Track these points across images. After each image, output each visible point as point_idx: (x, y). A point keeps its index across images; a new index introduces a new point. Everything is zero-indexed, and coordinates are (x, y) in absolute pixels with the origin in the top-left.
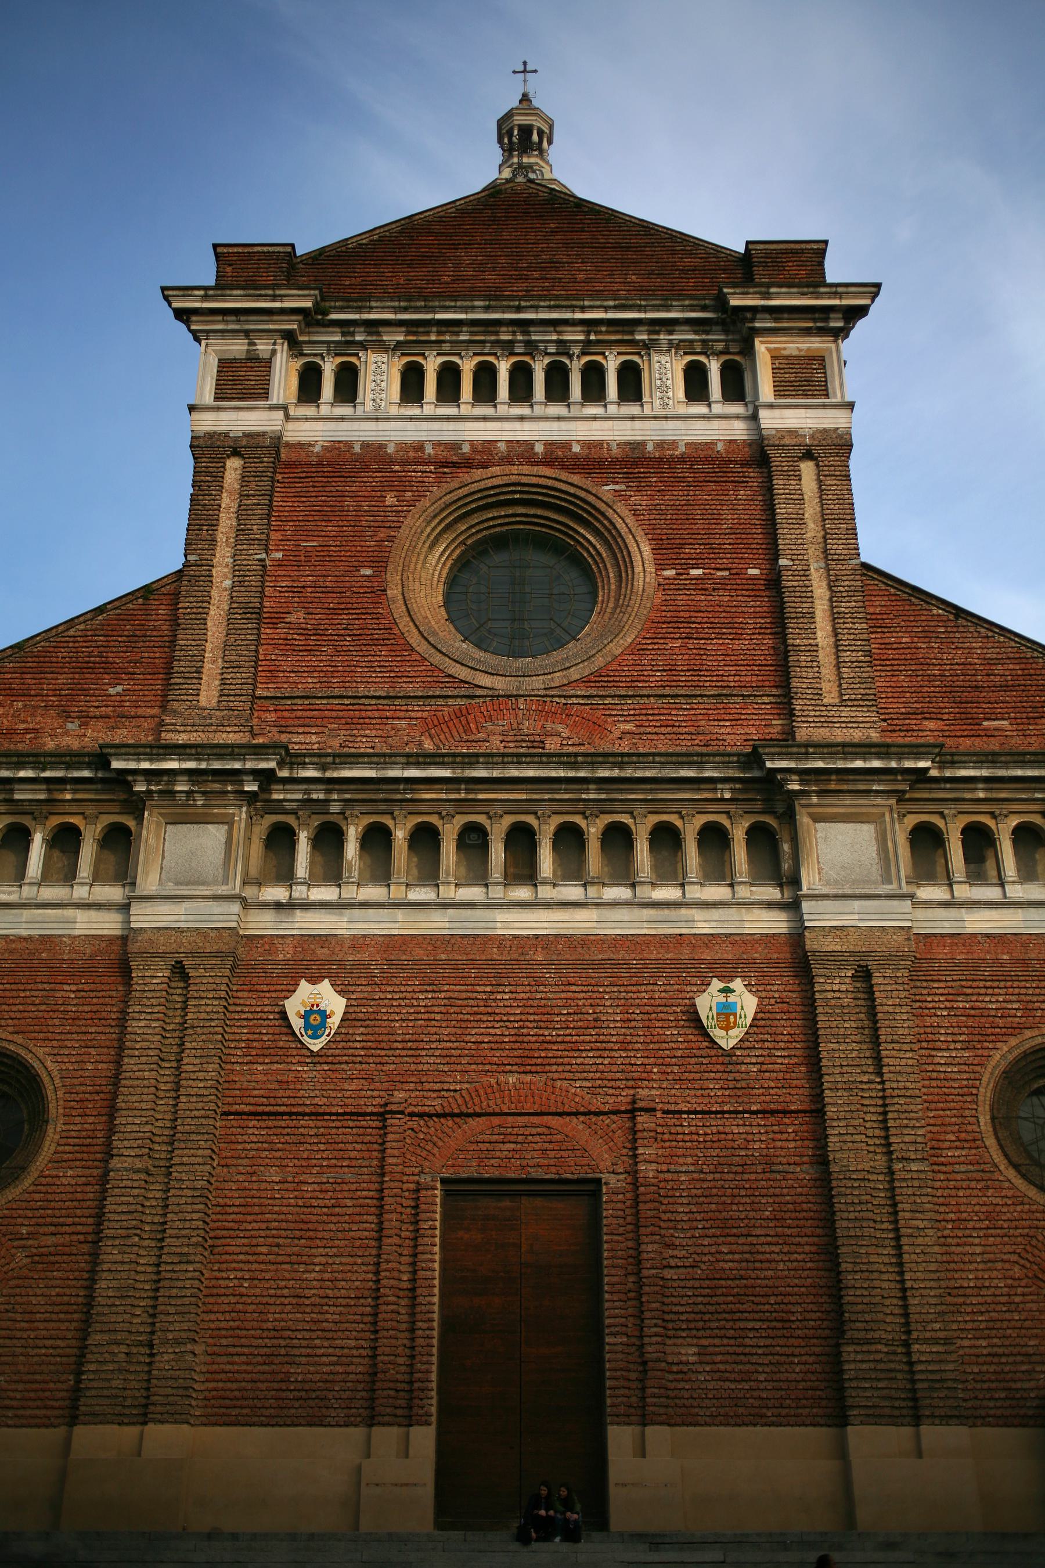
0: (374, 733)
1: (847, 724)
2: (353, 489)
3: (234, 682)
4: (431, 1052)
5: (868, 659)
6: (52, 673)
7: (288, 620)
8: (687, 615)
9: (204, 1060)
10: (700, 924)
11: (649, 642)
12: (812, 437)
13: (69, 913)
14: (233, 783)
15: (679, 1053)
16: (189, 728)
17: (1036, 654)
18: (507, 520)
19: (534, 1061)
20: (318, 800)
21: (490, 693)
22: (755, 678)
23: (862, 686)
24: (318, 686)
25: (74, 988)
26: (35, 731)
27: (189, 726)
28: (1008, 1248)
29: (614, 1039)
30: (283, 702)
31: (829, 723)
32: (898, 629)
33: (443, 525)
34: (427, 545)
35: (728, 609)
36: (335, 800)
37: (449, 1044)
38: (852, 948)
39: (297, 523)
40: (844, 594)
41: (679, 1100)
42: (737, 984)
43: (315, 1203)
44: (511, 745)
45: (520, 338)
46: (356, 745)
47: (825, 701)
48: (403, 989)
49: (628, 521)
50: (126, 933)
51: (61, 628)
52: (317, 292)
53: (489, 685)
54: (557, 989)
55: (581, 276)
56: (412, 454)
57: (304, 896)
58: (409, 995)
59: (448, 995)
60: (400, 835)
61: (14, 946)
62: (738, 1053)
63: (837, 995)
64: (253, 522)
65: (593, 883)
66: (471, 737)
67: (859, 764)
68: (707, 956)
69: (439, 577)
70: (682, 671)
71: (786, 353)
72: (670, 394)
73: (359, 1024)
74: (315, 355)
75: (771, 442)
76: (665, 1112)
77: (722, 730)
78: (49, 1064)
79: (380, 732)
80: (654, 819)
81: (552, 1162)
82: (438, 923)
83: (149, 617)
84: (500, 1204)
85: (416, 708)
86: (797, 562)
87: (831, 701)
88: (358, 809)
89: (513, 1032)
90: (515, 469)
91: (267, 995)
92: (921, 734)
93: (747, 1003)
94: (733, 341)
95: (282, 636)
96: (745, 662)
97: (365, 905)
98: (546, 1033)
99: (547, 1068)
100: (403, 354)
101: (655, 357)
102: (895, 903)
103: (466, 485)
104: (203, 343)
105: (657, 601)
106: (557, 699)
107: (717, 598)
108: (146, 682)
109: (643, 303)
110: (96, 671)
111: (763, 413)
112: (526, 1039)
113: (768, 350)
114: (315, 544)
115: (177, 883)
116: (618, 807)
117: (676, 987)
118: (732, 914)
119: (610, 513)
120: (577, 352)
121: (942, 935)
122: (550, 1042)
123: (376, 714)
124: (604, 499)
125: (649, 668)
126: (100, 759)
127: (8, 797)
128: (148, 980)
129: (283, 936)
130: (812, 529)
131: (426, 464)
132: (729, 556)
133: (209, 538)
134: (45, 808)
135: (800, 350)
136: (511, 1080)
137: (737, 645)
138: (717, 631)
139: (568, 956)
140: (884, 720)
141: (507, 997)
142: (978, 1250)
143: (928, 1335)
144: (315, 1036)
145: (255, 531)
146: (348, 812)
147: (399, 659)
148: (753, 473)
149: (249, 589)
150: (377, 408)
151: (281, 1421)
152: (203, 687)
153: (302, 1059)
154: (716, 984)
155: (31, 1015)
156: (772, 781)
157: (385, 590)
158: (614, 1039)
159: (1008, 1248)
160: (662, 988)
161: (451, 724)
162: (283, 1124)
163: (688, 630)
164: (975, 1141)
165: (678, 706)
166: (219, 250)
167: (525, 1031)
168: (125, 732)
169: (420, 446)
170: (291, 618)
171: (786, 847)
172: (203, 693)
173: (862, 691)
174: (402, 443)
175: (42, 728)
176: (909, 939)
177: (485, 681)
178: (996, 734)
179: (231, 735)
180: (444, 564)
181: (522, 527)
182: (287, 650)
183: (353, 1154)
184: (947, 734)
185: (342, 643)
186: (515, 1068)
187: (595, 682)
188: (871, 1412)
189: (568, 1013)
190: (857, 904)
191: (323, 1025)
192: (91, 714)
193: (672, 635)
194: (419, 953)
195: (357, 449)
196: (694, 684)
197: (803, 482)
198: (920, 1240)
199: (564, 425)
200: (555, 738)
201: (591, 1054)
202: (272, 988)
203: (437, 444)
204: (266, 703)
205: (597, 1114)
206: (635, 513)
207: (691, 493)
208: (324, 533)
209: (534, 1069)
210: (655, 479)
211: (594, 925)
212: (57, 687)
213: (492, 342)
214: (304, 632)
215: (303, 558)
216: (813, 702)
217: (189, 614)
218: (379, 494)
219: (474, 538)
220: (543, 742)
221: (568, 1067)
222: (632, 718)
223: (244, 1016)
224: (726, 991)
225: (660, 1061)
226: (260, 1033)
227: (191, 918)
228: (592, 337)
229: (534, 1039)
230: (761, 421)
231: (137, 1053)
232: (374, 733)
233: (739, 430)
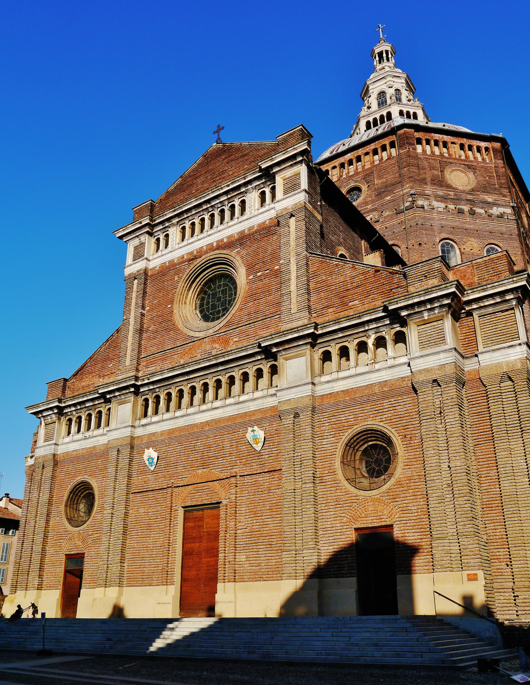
10: (251, 407)
17: (369, 269)
25: (101, 460)
28: (342, 512)
29: (227, 453)
41: (244, 471)
42: (256, 428)
43: (152, 518)
44: (203, 356)
48: (174, 446)
52: (148, 217)
56: (181, 260)
62: (262, 451)
71: (287, 177)
76: (240, 476)
81: (209, 497)
84: (199, 513)
88: (163, 389)
90: (208, 255)
92: (327, 315)
93: (261, 434)
100: (180, 225)
102: (306, 386)
105: (247, 289)
106: (216, 335)
109: (238, 179)
113: (281, 178)
121: (327, 394)
129: (144, 435)
131: (185, 262)
134: (94, 407)
135: (291, 174)
136: (200, 471)
137: (269, 298)
142: (332, 513)
143: (308, 547)
144: (151, 466)
151: (144, 585)
154: (250, 429)
158: (227, 453)
159: (342, 512)
160: (241, 432)
162: (145, 494)
169: (183, 257)
172: (127, 361)
176: (310, 399)
177: (197, 334)
178: (353, 307)
181: (216, 273)
183: (161, 502)
184: (336, 312)
188: (288, 575)
190: (294, 390)
191: (153, 462)
194: (177, 434)
195: (167, 264)
198: (308, 512)
201: (221, 459)
203: (188, 253)
205: (221, 480)
206: (242, 258)
213: (202, 211)
219: (204, 282)
224: (253, 431)
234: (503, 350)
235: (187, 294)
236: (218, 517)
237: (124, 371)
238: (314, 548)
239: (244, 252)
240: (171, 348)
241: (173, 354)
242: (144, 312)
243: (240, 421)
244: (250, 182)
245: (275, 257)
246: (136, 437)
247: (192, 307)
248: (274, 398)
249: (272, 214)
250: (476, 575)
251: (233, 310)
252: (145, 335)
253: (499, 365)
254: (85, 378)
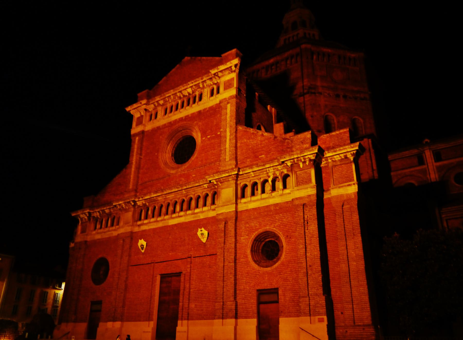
42: (203, 229)
67: (224, 175)
76: (194, 257)
82: (160, 225)
93: (206, 233)
94: (218, 80)
121: (244, 210)
144: (143, 250)
154: (199, 230)
164: (246, 257)
169: (165, 125)
191: (143, 247)
206: (199, 126)
224: (201, 231)
234: (344, 188)
235: (167, 147)
236: (180, 281)
238: (233, 301)
239: (200, 123)
242: (141, 157)
245: (218, 127)
247: (170, 155)
248: (214, 212)
249: (218, 101)
250: (323, 318)
251: (193, 158)
252: (141, 171)
253: (342, 196)
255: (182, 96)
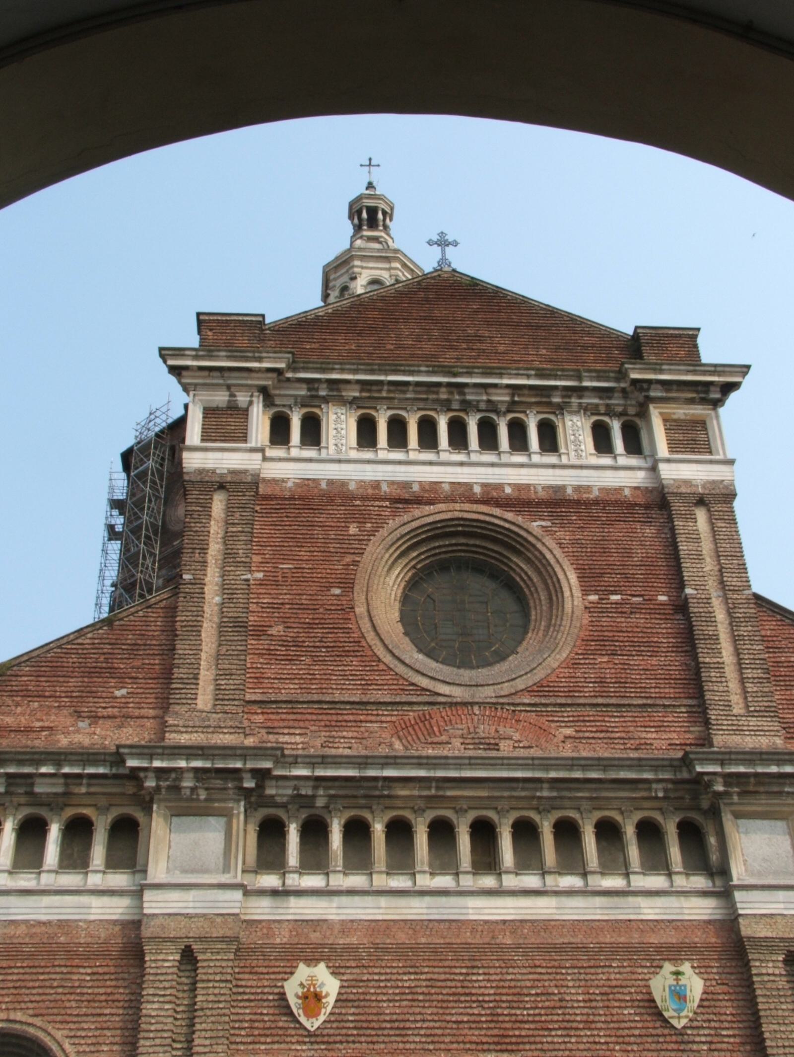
0: (350, 734)
1: (757, 732)
2: (321, 520)
3: (228, 687)
4: (416, 1032)
5: (767, 676)
6: (64, 676)
7: (269, 633)
8: (611, 634)
9: (214, 1041)
10: (646, 911)
11: (581, 657)
12: (703, 487)
13: (84, 899)
14: (234, 780)
15: (637, 1032)
16: (190, 729)
18: (450, 549)
19: (507, 1040)
20: (306, 796)
21: (449, 700)
22: (672, 690)
23: (765, 699)
24: (299, 691)
25: (89, 971)
26: (50, 728)
27: (189, 729)
29: (578, 1018)
30: (269, 706)
31: (739, 731)
32: (786, 650)
33: (398, 552)
34: (386, 569)
35: (645, 630)
36: (321, 796)
37: (432, 1024)
38: (781, 935)
39: (274, 548)
40: (742, 620)
42: (686, 967)
45: (457, 397)
46: (336, 745)
47: (735, 712)
48: (388, 971)
49: (555, 552)
50: (136, 918)
51: (72, 637)
52: (290, 355)
53: (447, 693)
54: (524, 971)
55: (501, 348)
56: (370, 491)
57: (296, 883)
58: (394, 977)
59: (429, 976)
60: (378, 828)
61: (34, 930)
62: (689, 1032)
63: (772, 978)
64: (239, 547)
65: (550, 873)
66: (435, 740)
67: (774, 769)
68: (654, 939)
69: (396, 596)
70: (611, 683)
71: (675, 417)
72: (583, 447)
73: (350, 1004)
74: (284, 406)
75: (671, 490)
77: (649, 736)
78: (67, 1046)
79: (355, 734)
80: (598, 815)
83: (149, 628)
85: (386, 713)
86: (701, 592)
87: (742, 712)
88: (339, 805)
89: (488, 1012)
90: (457, 506)
91: (267, 977)
94: (631, 405)
95: (266, 647)
96: (663, 677)
97: (351, 892)
98: (518, 1012)
99: (521, 1047)
101: (567, 418)
103: (418, 518)
104: (191, 393)
105: (585, 622)
107: (634, 620)
108: (148, 686)
110: (103, 675)
111: (662, 466)
112: (501, 1019)
113: (661, 414)
114: (290, 566)
115: (184, 871)
116: (567, 803)
117: (628, 969)
118: (672, 902)
119: (539, 546)
120: (503, 409)
122: (521, 1022)
123: (351, 718)
124: (535, 533)
125: (582, 680)
126: (117, 758)
127: (28, 789)
128: (160, 964)
130: (709, 565)
132: (641, 584)
133: (201, 559)
134: (61, 800)
137: (654, 661)
138: (637, 648)
139: (533, 940)
140: (784, 728)
141: (481, 978)
145: (241, 555)
146: (332, 806)
147: (368, 668)
148: (655, 513)
149: (238, 605)
150: (339, 451)
152: (200, 692)
153: (301, 1039)
154: (668, 967)
155: (49, 997)
156: (699, 783)
157: (353, 608)
160: (616, 970)
161: (416, 727)
163: (613, 648)
165: (610, 714)
166: (202, 317)
167: (499, 1011)
168: (130, 730)
169: (376, 485)
170: (273, 631)
171: (712, 840)
172: (200, 697)
173: (766, 704)
174: (362, 481)
175: (57, 727)
179: (227, 736)
180: (399, 585)
181: (463, 554)
182: (271, 659)
185: (318, 654)
186: (492, 1047)
187: (538, 691)
189: (537, 994)
192: (100, 714)
193: (599, 652)
194: (402, 937)
195: (324, 485)
196: (622, 694)
197: (698, 524)
199: (497, 470)
200: (508, 741)
201: (559, 1033)
202: (271, 970)
203: (392, 483)
204: (255, 708)
207: (606, 530)
208: (297, 558)
209: (509, 1047)
210: (574, 518)
211: (554, 911)
212: (69, 689)
214: (284, 643)
215: (280, 578)
216: (725, 713)
217: (185, 626)
218: (343, 524)
220: (497, 744)
221: (539, 1046)
222: (572, 724)
223: (246, 997)
225: (621, 1040)
226: (262, 1014)
227: (198, 905)
228: (516, 399)
229: (507, 1019)
230: (661, 473)
231: (152, 1035)
232: (350, 734)
233: (639, 478)
237: (197, 724)
240: (357, 700)
241: (362, 718)
243: (613, 940)
244: (579, 391)
246: (245, 921)
254: (10, 703)
255: (455, 406)
